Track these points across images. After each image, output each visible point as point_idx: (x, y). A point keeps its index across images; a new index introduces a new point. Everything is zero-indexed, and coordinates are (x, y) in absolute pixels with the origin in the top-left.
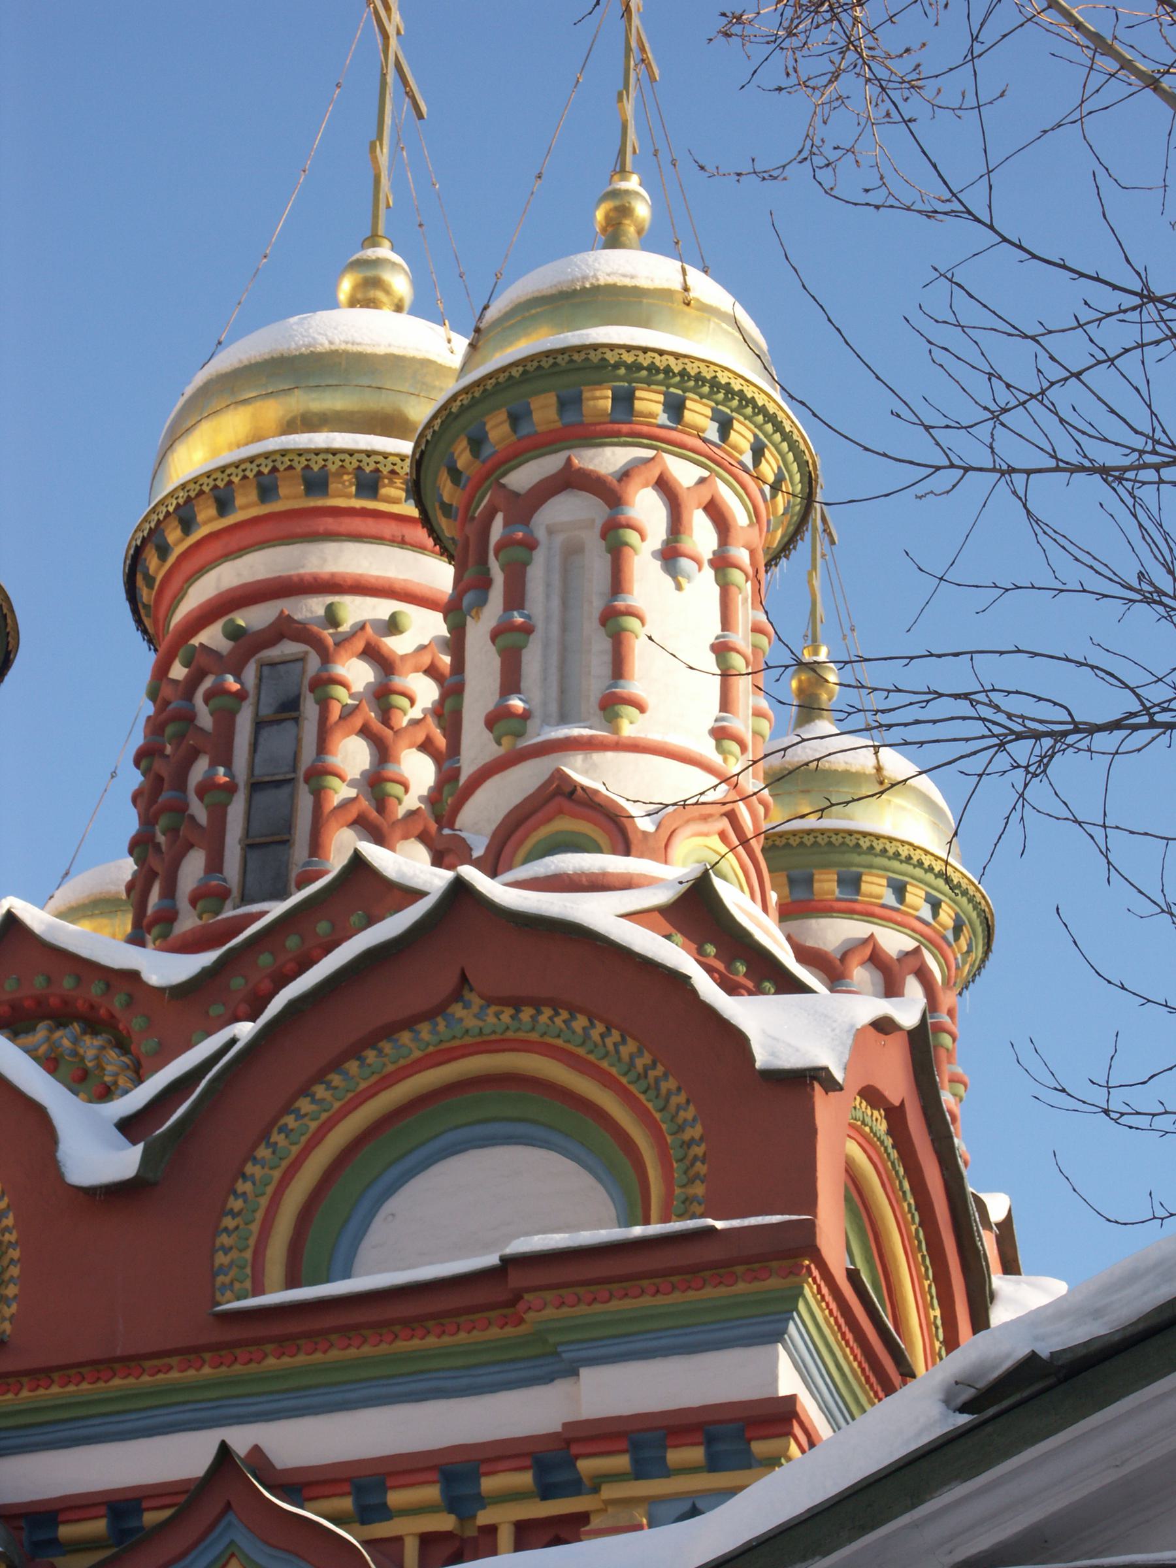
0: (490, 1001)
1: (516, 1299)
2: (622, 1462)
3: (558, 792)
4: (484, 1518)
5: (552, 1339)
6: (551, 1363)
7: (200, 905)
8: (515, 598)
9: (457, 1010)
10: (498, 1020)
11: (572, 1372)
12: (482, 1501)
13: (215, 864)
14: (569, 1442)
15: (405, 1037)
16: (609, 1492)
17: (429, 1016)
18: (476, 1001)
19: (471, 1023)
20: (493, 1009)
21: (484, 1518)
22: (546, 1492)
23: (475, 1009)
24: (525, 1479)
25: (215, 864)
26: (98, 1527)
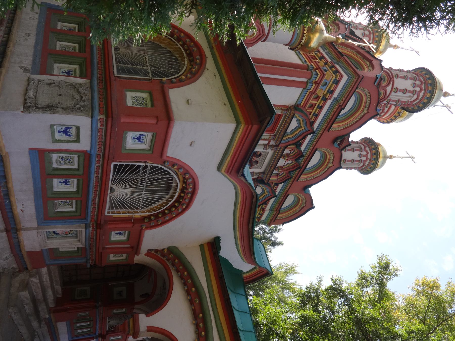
8: (357, 161)
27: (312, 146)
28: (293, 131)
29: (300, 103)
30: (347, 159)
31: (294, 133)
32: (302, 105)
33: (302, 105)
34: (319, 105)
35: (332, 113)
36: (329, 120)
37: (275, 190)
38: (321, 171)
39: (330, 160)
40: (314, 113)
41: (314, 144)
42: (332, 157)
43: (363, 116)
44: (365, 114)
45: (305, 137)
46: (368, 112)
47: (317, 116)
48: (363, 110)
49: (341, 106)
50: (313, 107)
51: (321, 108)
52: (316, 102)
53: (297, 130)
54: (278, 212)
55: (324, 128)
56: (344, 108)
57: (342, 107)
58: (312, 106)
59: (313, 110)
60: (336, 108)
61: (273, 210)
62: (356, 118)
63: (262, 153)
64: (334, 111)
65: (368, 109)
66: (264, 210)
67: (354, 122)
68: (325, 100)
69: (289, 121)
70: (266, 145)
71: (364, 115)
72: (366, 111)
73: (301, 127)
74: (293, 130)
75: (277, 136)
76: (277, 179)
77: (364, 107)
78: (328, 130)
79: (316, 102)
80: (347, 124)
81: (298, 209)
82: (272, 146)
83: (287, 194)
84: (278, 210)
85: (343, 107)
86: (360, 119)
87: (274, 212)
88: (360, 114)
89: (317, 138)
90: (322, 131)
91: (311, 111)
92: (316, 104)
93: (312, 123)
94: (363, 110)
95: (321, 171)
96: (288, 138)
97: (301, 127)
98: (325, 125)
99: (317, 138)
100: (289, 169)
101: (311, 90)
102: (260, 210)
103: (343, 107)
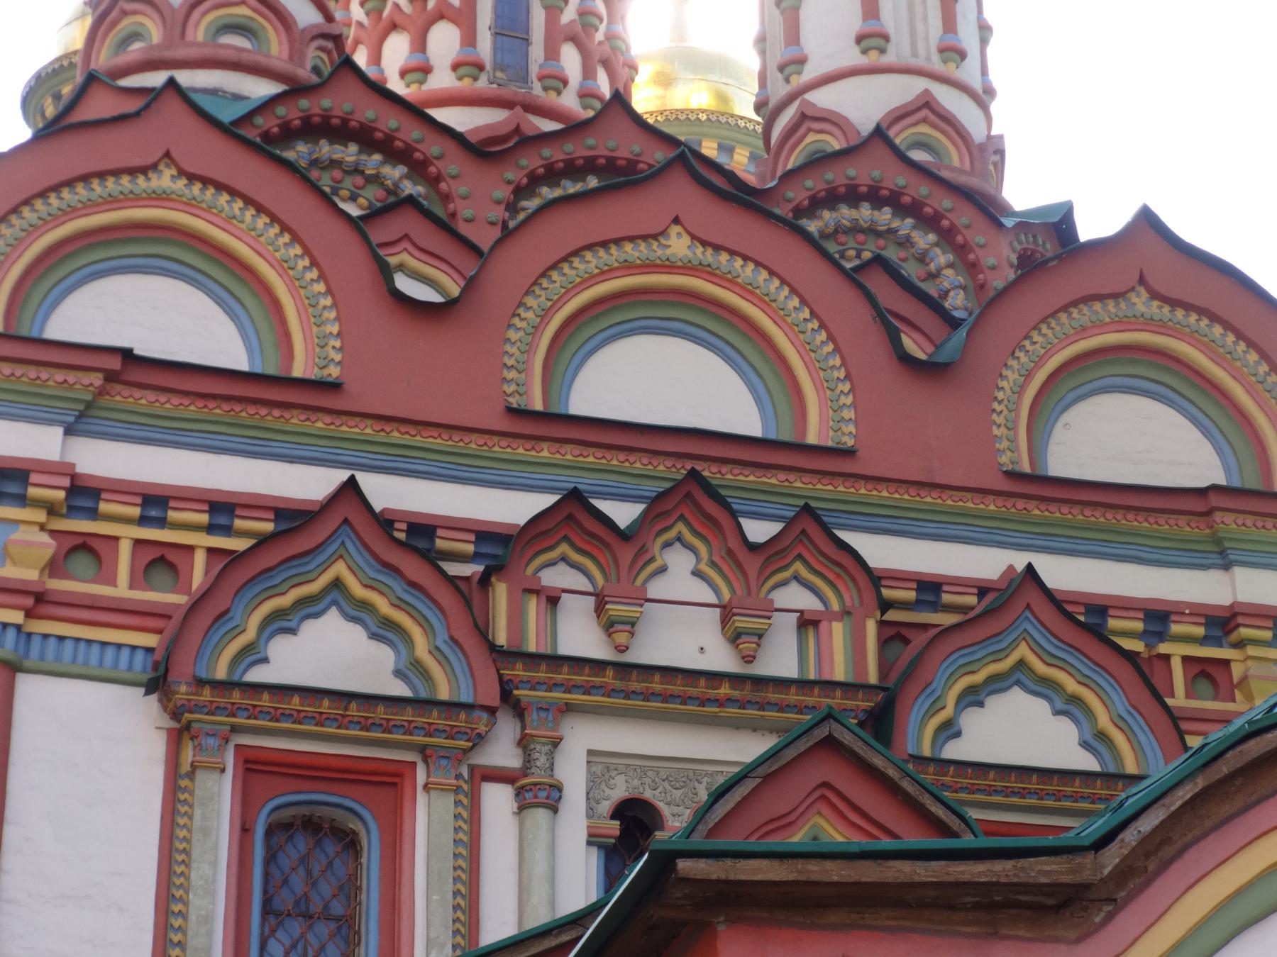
0: (1154, 295)
1: (1208, 513)
2: (1268, 635)
3: (927, 105)
4: (1163, 648)
5: (1227, 544)
6: (1222, 557)
7: (462, 70)
9: (1134, 298)
10: (1156, 310)
11: (1227, 567)
12: (1162, 636)
13: (469, 39)
14: (1235, 615)
15: (1097, 306)
16: (1252, 651)
17: (1116, 296)
18: (1144, 294)
19: (1141, 308)
20: (1156, 303)
21: (1163, 648)
22: (1204, 641)
23: (1144, 299)
24: (1200, 631)
25: (469, 39)
26: (911, 595)
27: (499, 448)
28: (385, 631)
29: (140, 655)
30: (854, 22)
31: (388, 623)
32: (150, 640)
33: (150, 640)
34: (143, 521)
35: (193, 409)
36: (245, 413)
37: (983, 589)
38: (747, 291)
39: (628, 268)
40: (211, 529)
41: (474, 444)
42: (592, 262)
43: (206, 181)
44: (182, 173)
45: (421, 533)
46: (167, 155)
47: (222, 509)
48: (161, 198)
49: (111, 377)
50: (171, 556)
51: (155, 502)
52: (125, 549)
53: (365, 605)
54: (1215, 500)
55: (321, 424)
56: (127, 354)
57: (127, 366)
58: (160, 562)
59: (190, 549)
60: (145, 399)
61: (1218, 541)
62: (228, 223)
63: (619, 791)
64: (169, 405)
65: (144, 170)
66: (1222, 623)
67: (263, 220)
68: (84, 493)
69: (265, 700)
70: (519, 793)
71: (192, 178)
72: (165, 180)
73: (337, 584)
74: (374, 636)
75: (419, 739)
76: (846, 613)
77: (135, 199)
78: (333, 387)
79: (125, 549)
80: (283, 267)
81: (1193, 338)
82: (524, 743)
83: (1006, 485)
84: (1199, 506)
85: (115, 363)
86: (234, 193)
87: (1228, 523)
88: (190, 206)
89: (418, 440)
90: (347, 428)
91: (200, 558)
92: (138, 542)
93: (293, 518)
94: (161, 198)
95: (747, 291)
96: (436, 651)
97: (337, 584)
98: (296, 420)
99: (418, 440)
100: (730, 553)
101: (17, 617)
102: (1240, 644)
103: (115, 363)
